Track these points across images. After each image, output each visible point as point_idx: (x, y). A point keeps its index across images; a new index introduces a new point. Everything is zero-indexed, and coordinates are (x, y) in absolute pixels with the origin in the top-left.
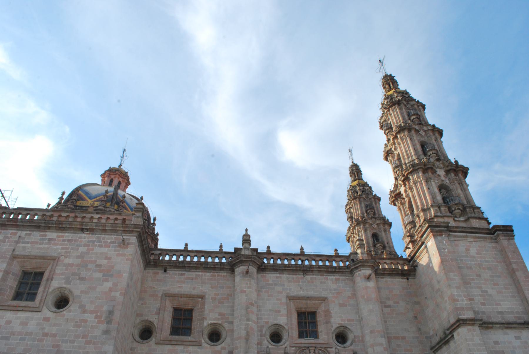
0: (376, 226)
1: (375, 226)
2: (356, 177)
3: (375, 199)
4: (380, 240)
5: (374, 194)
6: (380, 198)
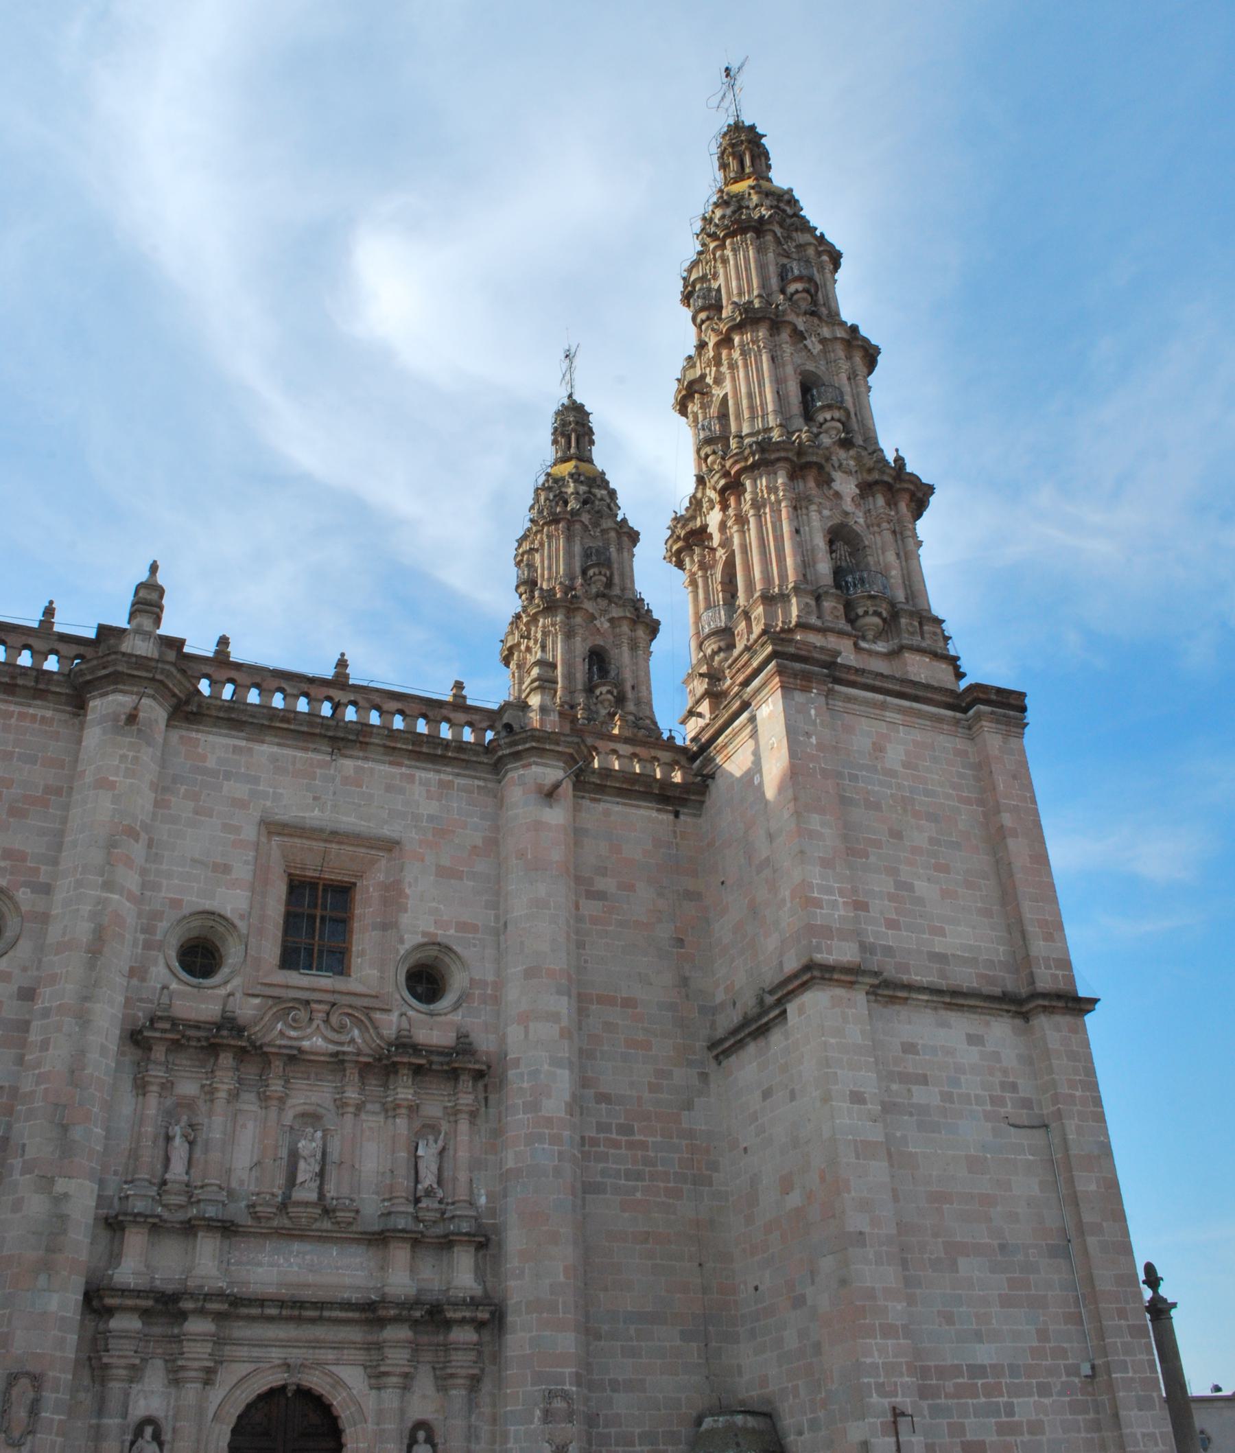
0: (607, 625)
1: (603, 624)
2: (573, 451)
4: (613, 674)
5: (619, 519)
6: (637, 534)
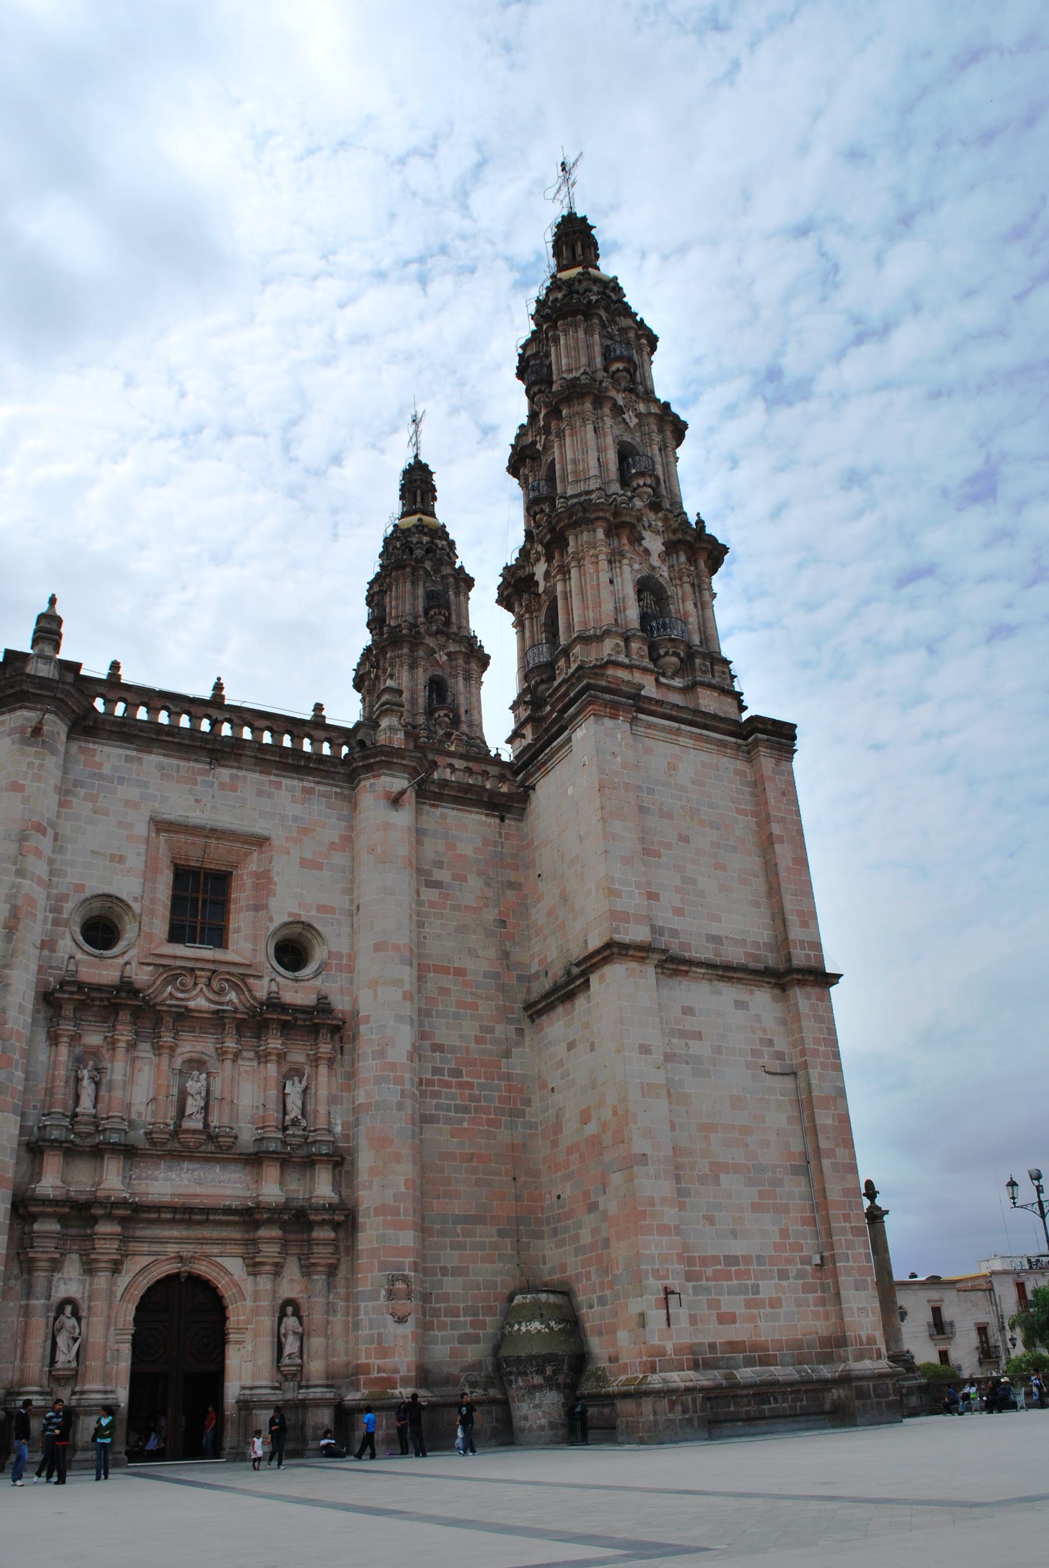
0: (445, 658)
2: (419, 505)
3: (457, 581)
4: (449, 700)
5: (457, 566)
6: (473, 580)
